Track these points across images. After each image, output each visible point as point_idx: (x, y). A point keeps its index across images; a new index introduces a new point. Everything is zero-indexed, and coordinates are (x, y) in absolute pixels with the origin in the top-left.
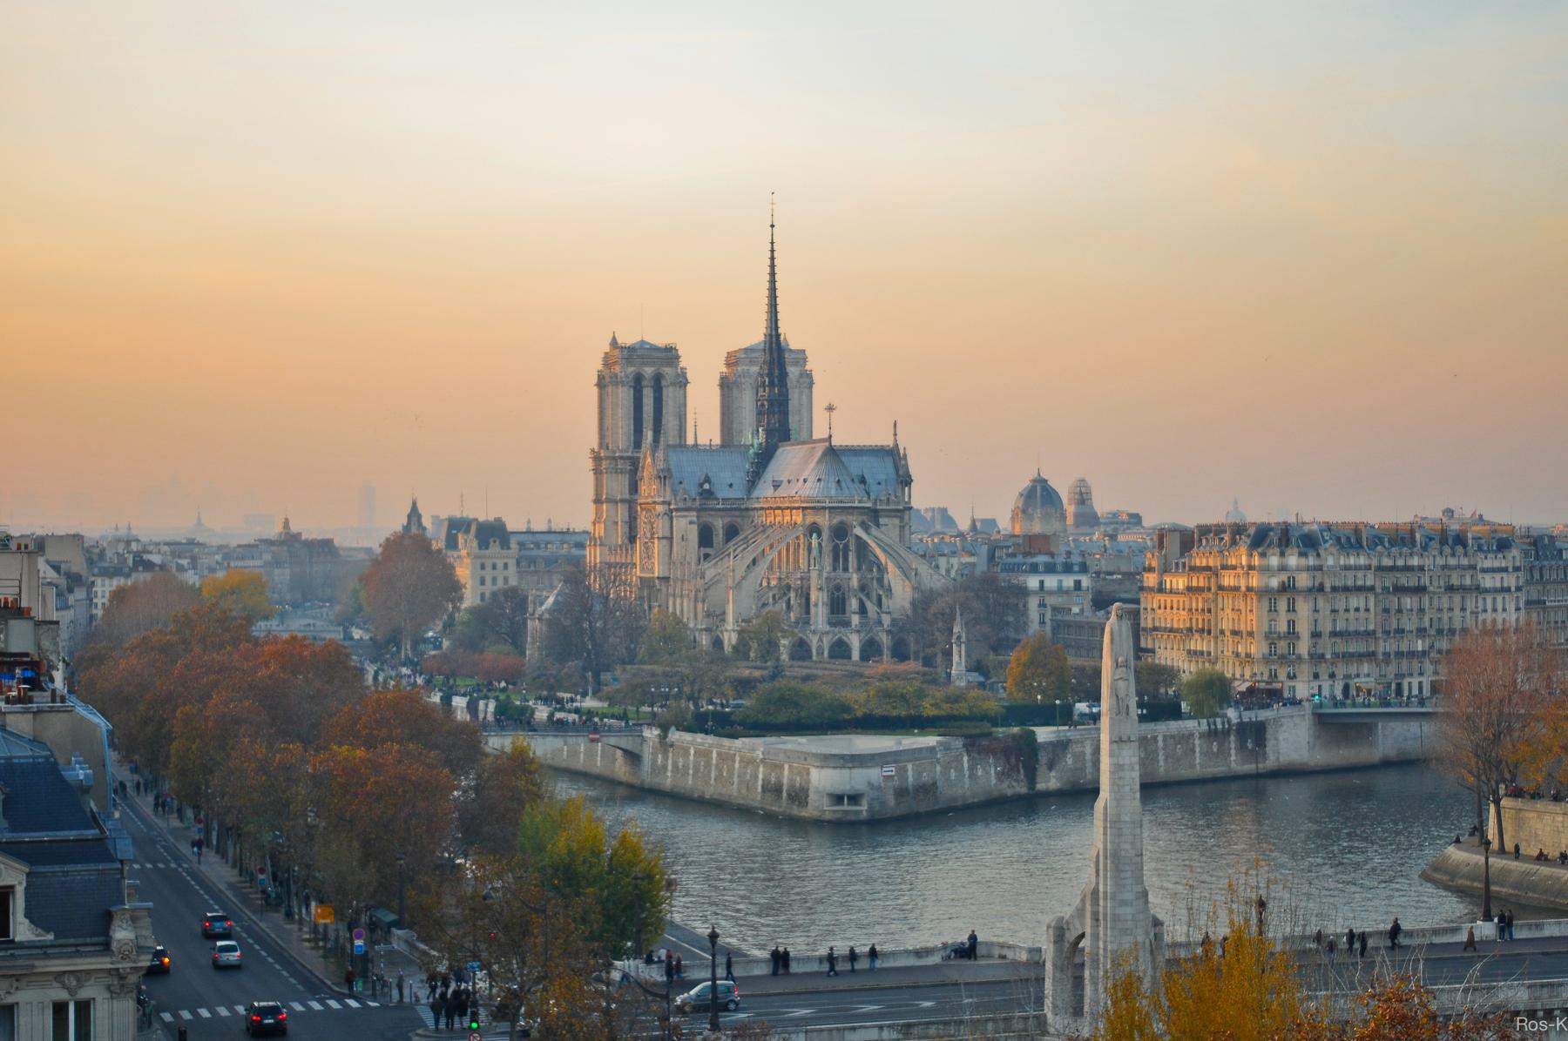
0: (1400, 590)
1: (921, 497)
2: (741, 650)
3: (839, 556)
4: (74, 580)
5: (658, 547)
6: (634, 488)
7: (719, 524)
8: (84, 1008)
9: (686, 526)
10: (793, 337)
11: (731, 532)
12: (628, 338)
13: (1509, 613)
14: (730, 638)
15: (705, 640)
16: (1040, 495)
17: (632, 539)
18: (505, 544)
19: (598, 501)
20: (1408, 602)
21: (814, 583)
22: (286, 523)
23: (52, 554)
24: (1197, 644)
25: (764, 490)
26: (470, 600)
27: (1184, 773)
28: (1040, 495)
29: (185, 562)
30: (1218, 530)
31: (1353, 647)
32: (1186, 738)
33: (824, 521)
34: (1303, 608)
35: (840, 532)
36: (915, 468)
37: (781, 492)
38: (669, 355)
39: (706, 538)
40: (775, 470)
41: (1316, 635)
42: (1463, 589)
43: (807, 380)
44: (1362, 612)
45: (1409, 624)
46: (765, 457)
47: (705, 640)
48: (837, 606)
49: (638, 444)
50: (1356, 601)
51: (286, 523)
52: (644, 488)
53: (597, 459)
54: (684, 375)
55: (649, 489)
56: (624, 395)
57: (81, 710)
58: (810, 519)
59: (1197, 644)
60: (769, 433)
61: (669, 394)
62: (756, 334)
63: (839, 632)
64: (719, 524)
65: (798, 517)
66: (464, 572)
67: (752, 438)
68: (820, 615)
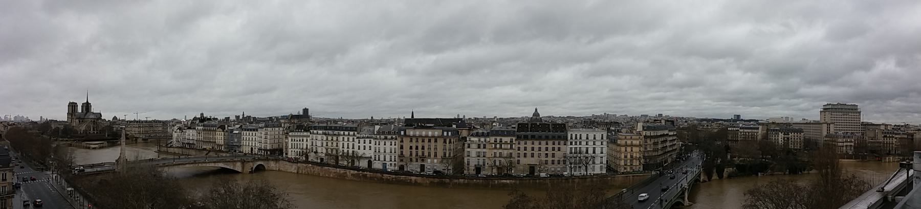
1: (103, 118)
2: (83, 133)
3: (94, 124)
4: (5, 126)
5: (74, 123)
7: (81, 120)
8: (6, 174)
9: (77, 120)
12: (71, 102)
13: (160, 129)
14: (82, 132)
15: (79, 132)
16: (115, 118)
19: (68, 118)
23: (3, 123)
26: (53, 128)
28: (115, 118)
33: (93, 120)
34: (141, 128)
35: (94, 121)
36: (102, 115)
38: (76, 103)
39: (80, 122)
40: (87, 115)
43: (91, 106)
44: (147, 129)
46: (86, 113)
47: (79, 132)
48: (93, 128)
56: (71, 107)
57: (7, 141)
61: (76, 107)
62: (86, 101)
64: (81, 120)
67: (85, 112)
68: (92, 130)
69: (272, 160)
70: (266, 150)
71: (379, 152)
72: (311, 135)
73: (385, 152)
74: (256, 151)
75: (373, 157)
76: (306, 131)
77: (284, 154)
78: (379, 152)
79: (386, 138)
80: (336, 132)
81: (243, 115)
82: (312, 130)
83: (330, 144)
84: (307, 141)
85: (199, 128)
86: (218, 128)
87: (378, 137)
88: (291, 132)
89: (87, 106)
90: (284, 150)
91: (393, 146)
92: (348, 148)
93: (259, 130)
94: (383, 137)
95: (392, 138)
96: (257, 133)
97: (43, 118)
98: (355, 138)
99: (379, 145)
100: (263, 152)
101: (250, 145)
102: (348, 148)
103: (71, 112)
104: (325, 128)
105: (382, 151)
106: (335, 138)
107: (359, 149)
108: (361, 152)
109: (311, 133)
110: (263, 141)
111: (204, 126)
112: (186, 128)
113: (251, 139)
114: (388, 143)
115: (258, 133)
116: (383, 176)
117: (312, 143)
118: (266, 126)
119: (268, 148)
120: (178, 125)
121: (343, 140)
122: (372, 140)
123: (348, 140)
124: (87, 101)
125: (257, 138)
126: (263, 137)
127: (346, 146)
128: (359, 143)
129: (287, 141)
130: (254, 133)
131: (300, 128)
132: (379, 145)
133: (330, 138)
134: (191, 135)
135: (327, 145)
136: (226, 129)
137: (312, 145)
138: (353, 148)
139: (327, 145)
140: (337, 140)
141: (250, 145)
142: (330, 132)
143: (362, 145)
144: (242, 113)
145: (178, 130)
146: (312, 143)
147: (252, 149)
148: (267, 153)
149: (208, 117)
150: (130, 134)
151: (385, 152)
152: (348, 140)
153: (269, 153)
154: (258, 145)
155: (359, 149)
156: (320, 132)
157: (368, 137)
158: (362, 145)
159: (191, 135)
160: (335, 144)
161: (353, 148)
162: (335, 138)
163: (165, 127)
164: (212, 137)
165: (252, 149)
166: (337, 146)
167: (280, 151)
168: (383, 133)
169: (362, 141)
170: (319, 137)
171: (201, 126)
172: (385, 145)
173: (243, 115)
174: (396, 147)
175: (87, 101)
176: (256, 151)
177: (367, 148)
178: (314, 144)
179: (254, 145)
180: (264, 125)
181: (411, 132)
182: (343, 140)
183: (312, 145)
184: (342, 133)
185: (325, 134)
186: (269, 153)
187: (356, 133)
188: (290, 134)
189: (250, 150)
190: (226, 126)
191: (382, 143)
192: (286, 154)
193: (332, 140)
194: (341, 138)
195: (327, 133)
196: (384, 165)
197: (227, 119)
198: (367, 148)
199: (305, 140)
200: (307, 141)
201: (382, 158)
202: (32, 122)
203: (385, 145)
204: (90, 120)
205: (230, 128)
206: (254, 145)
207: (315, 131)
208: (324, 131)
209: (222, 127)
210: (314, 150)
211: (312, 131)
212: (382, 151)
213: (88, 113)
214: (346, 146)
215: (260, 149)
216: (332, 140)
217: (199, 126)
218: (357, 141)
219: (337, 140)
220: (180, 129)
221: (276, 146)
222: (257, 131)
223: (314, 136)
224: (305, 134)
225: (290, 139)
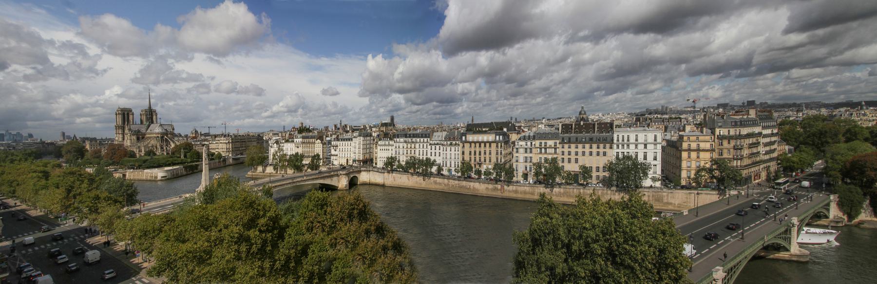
0: (242, 142)
5: (129, 141)
6: (124, 131)
9: (134, 138)
10: (153, 108)
11: (143, 138)
12: (122, 107)
17: (124, 139)
18: (96, 142)
20: (243, 143)
21: (158, 145)
22: (41, 140)
24: (217, 150)
25: (149, 131)
27: (220, 166)
29: (11, 148)
30: (220, 135)
31: (237, 149)
32: (216, 163)
35: (162, 137)
37: (152, 131)
38: (130, 110)
41: (232, 148)
42: (250, 141)
45: (243, 146)
46: (149, 126)
49: (124, 124)
50: (237, 143)
51: (41, 140)
52: (126, 131)
53: (116, 127)
54: (133, 113)
55: (126, 131)
58: (157, 135)
59: (217, 150)
60: (149, 122)
63: (163, 152)
65: (155, 135)
66: (88, 147)
69: (365, 171)
70: (359, 161)
71: (446, 158)
72: (395, 144)
73: (451, 158)
74: (350, 163)
75: (442, 165)
76: (391, 139)
77: (374, 165)
78: (446, 158)
79: (451, 144)
80: (414, 140)
81: (341, 124)
82: (395, 138)
83: (409, 152)
84: (392, 150)
85: (298, 140)
86: (317, 140)
87: (445, 143)
88: (380, 140)
89: (150, 115)
90: (374, 160)
91: (457, 152)
92: (423, 155)
93: (353, 139)
94: (449, 143)
95: (456, 144)
96: (352, 143)
97: (66, 134)
98: (428, 144)
99: (446, 150)
100: (357, 162)
101: (346, 156)
102: (423, 155)
103: (120, 123)
104: (406, 136)
105: (448, 157)
106: (413, 146)
107: (431, 156)
108: (432, 158)
109: (395, 142)
110: (357, 151)
111: (303, 138)
112: (283, 141)
113: (346, 150)
114: (453, 148)
115: (353, 143)
116: (449, 182)
117: (396, 151)
118: (360, 136)
119: (361, 159)
120: (275, 138)
121: (420, 148)
122: (441, 146)
123: (423, 147)
124: (150, 107)
125: (352, 148)
126: (357, 147)
127: (421, 154)
128: (431, 149)
129: (376, 150)
130: (349, 143)
131: (386, 136)
132: (446, 150)
133: (409, 146)
134: (289, 149)
135: (407, 153)
136: (324, 139)
137: (396, 154)
138: (427, 155)
139: (407, 153)
140: (415, 147)
141: (346, 156)
142: (410, 140)
143: (433, 151)
144: (340, 121)
145: (275, 144)
146: (396, 151)
147: (347, 159)
148: (360, 164)
149: (308, 127)
150: (216, 153)
151: (451, 158)
152: (423, 147)
153: (361, 163)
154: (352, 155)
155: (431, 156)
156: (402, 140)
157: (438, 144)
158: (433, 151)
159: (289, 149)
160: (413, 152)
161: (427, 155)
162: (413, 146)
163: (260, 142)
164: (311, 150)
165: (347, 159)
166: (414, 153)
167: (371, 160)
168: (450, 140)
169: (433, 147)
170: (401, 145)
171: (300, 138)
172: (451, 150)
173: (341, 124)
174: (459, 153)
175: (150, 107)
176: (350, 163)
177: (437, 154)
178: (398, 153)
179: (349, 156)
180: (357, 134)
181: (470, 138)
182: (420, 148)
183: (396, 154)
184: (418, 140)
185: (405, 142)
186: (361, 163)
187: (429, 139)
188: (379, 143)
189: (346, 161)
190: (324, 137)
191: (449, 148)
192: (376, 164)
193: (411, 147)
194: (417, 145)
195: (407, 141)
196: (450, 170)
197: (327, 128)
198: (437, 154)
199: (390, 150)
200: (392, 150)
201: (448, 165)
202: (42, 143)
203: (451, 150)
204: (155, 135)
205: (328, 139)
206: (349, 156)
207: (398, 140)
208: (405, 139)
209: (321, 138)
210: (398, 160)
211: (395, 139)
212: (448, 157)
213: (152, 125)
214: (421, 154)
215: (354, 161)
216: (411, 147)
217: (298, 138)
218: (429, 147)
219: (415, 147)
220: (277, 142)
221: (367, 156)
222: (352, 140)
223: (398, 144)
224: (391, 143)
225: (379, 148)
